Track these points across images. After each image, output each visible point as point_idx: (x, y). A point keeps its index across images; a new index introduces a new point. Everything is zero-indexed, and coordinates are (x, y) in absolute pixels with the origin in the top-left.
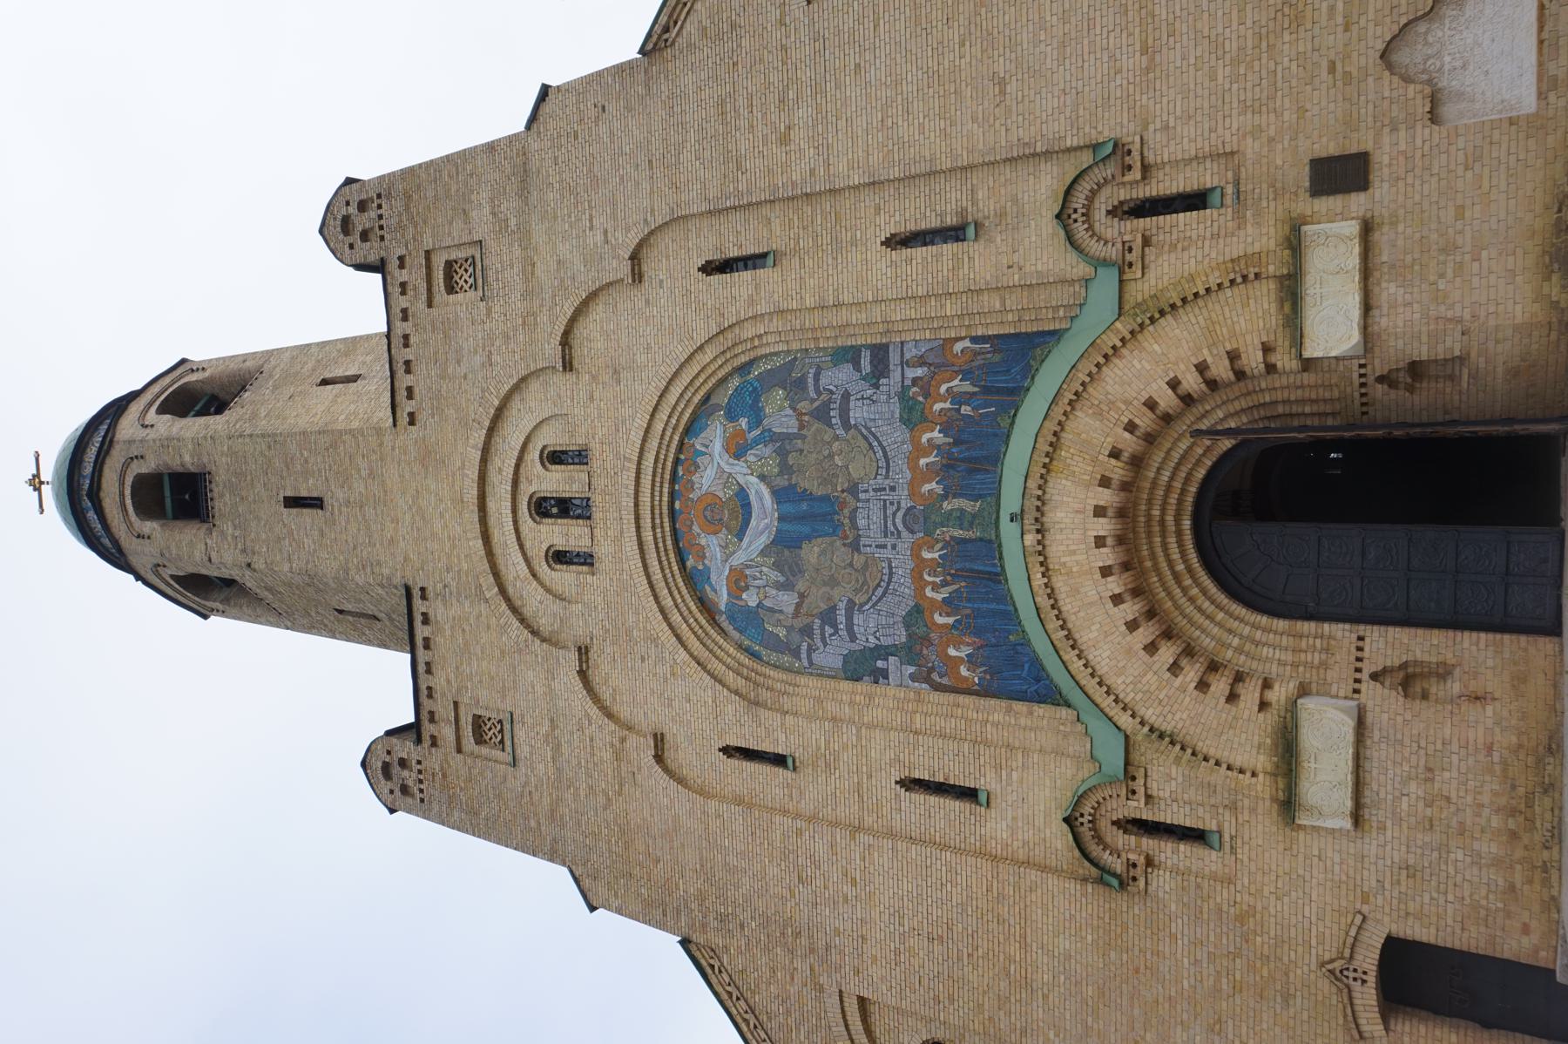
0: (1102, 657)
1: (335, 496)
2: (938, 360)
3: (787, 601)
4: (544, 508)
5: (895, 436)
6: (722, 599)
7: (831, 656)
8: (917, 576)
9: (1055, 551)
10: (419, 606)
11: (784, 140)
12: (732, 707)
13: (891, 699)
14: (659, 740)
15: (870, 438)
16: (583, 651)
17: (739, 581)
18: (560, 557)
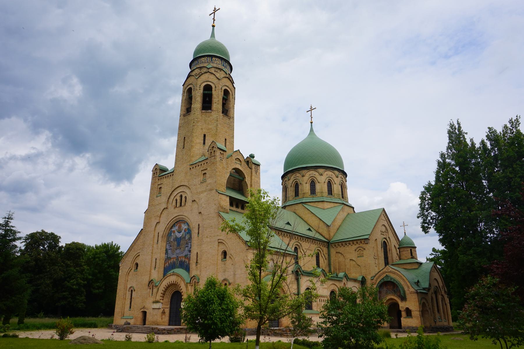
0: (164, 283)
1: (185, 151)
2: (189, 260)
3: (172, 240)
4: (181, 196)
5: (184, 254)
6: (173, 230)
7: (168, 247)
8: (173, 258)
9: (171, 277)
10: (172, 174)
11: (207, 237)
12: (162, 233)
13: (164, 256)
14: (159, 223)
15: (184, 250)
16: (167, 208)
17: (174, 232)
18: (177, 200)
